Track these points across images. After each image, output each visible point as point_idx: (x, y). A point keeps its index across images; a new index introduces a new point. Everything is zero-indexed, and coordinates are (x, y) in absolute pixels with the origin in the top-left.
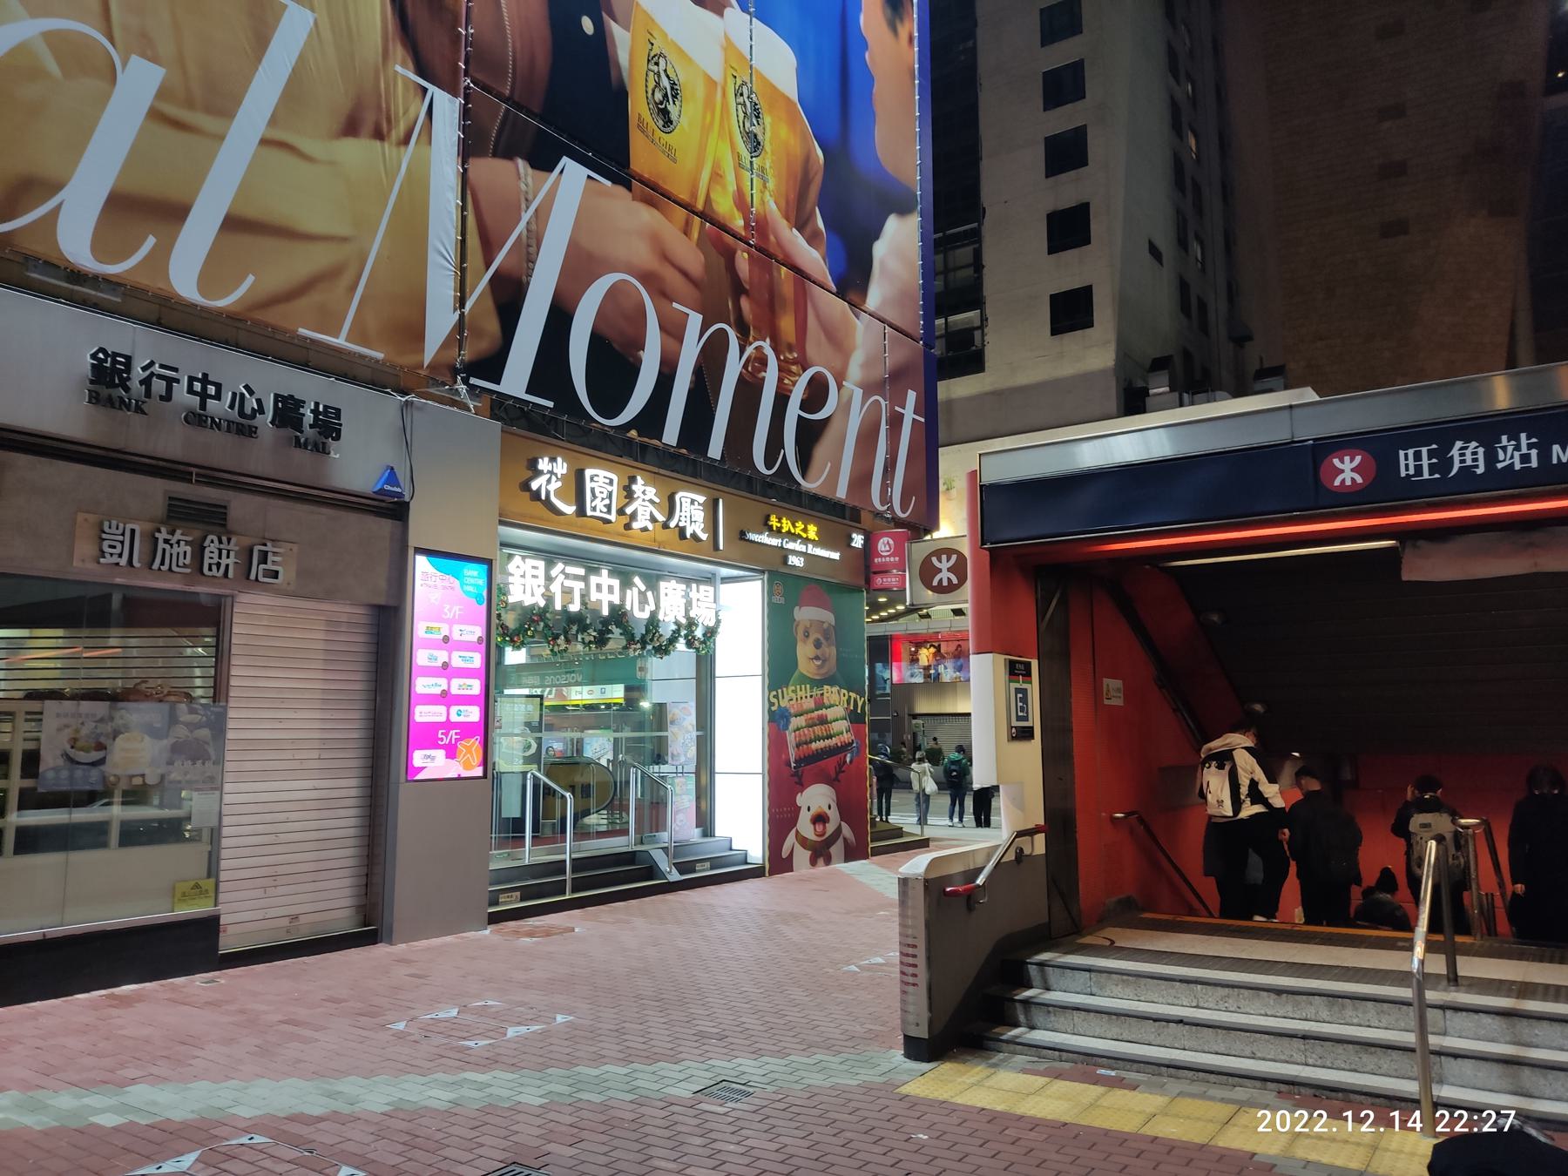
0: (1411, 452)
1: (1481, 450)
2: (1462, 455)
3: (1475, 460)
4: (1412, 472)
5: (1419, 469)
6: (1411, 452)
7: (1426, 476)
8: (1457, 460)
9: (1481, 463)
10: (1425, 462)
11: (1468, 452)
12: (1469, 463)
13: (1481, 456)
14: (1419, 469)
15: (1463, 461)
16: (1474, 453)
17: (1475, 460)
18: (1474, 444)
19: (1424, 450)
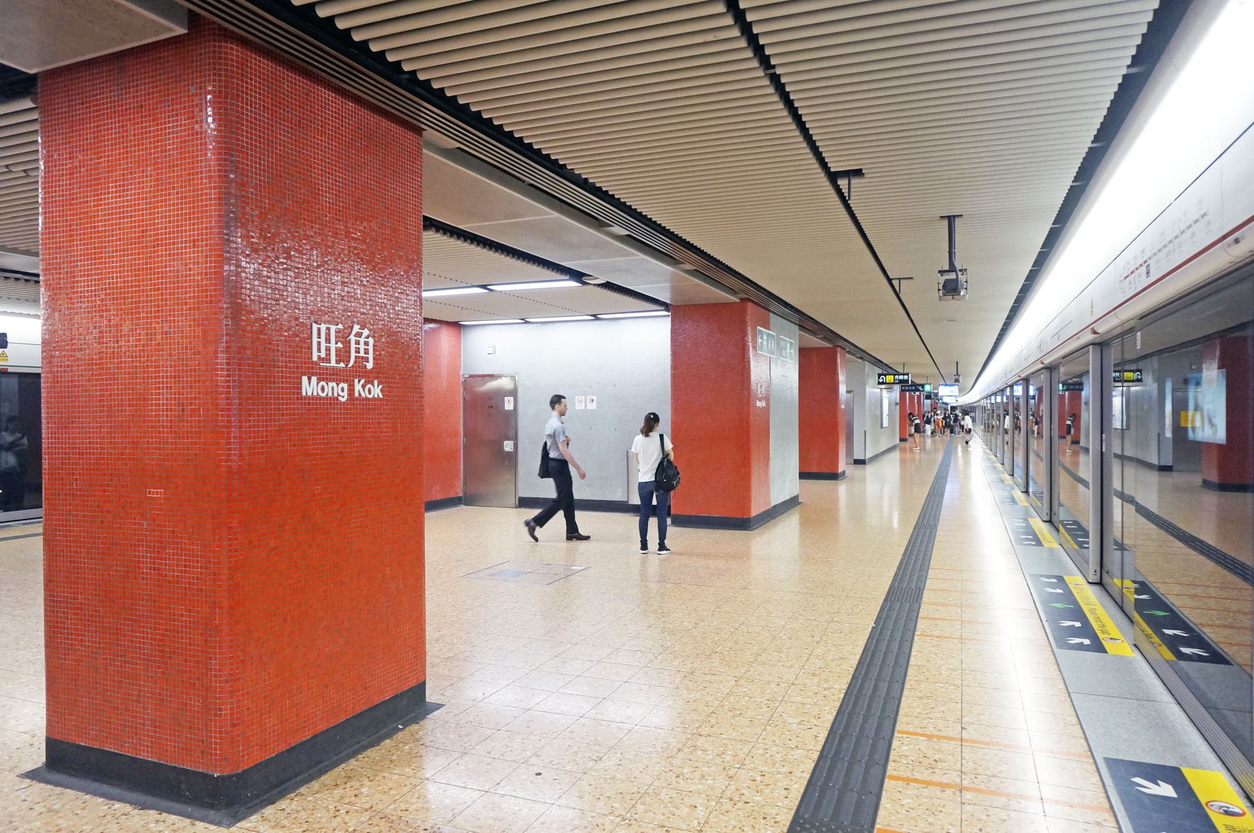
0: (323, 327)
1: (371, 341)
2: (358, 343)
3: (366, 352)
4: (323, 355)
5: (328, 349)
6: (323, 327)
7: (333, 363)
8: (353, 346)
9: (371, 356)
10: (333, 346)
11: (362, 340)
12: (362, 354)
13: (371, 348)
14: (328, 349)
15: (358, 351)
16: (366, 344)
17: (366, 352)
18: (366, 332)
19: (333, 328)
